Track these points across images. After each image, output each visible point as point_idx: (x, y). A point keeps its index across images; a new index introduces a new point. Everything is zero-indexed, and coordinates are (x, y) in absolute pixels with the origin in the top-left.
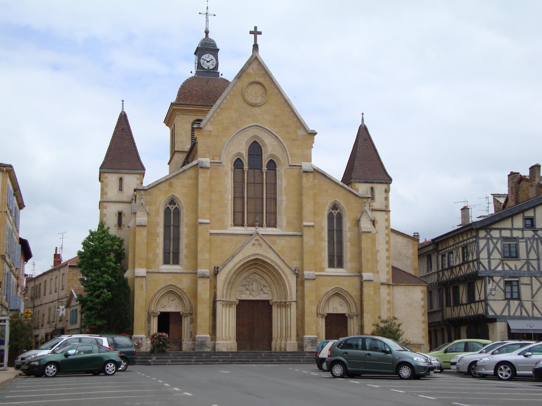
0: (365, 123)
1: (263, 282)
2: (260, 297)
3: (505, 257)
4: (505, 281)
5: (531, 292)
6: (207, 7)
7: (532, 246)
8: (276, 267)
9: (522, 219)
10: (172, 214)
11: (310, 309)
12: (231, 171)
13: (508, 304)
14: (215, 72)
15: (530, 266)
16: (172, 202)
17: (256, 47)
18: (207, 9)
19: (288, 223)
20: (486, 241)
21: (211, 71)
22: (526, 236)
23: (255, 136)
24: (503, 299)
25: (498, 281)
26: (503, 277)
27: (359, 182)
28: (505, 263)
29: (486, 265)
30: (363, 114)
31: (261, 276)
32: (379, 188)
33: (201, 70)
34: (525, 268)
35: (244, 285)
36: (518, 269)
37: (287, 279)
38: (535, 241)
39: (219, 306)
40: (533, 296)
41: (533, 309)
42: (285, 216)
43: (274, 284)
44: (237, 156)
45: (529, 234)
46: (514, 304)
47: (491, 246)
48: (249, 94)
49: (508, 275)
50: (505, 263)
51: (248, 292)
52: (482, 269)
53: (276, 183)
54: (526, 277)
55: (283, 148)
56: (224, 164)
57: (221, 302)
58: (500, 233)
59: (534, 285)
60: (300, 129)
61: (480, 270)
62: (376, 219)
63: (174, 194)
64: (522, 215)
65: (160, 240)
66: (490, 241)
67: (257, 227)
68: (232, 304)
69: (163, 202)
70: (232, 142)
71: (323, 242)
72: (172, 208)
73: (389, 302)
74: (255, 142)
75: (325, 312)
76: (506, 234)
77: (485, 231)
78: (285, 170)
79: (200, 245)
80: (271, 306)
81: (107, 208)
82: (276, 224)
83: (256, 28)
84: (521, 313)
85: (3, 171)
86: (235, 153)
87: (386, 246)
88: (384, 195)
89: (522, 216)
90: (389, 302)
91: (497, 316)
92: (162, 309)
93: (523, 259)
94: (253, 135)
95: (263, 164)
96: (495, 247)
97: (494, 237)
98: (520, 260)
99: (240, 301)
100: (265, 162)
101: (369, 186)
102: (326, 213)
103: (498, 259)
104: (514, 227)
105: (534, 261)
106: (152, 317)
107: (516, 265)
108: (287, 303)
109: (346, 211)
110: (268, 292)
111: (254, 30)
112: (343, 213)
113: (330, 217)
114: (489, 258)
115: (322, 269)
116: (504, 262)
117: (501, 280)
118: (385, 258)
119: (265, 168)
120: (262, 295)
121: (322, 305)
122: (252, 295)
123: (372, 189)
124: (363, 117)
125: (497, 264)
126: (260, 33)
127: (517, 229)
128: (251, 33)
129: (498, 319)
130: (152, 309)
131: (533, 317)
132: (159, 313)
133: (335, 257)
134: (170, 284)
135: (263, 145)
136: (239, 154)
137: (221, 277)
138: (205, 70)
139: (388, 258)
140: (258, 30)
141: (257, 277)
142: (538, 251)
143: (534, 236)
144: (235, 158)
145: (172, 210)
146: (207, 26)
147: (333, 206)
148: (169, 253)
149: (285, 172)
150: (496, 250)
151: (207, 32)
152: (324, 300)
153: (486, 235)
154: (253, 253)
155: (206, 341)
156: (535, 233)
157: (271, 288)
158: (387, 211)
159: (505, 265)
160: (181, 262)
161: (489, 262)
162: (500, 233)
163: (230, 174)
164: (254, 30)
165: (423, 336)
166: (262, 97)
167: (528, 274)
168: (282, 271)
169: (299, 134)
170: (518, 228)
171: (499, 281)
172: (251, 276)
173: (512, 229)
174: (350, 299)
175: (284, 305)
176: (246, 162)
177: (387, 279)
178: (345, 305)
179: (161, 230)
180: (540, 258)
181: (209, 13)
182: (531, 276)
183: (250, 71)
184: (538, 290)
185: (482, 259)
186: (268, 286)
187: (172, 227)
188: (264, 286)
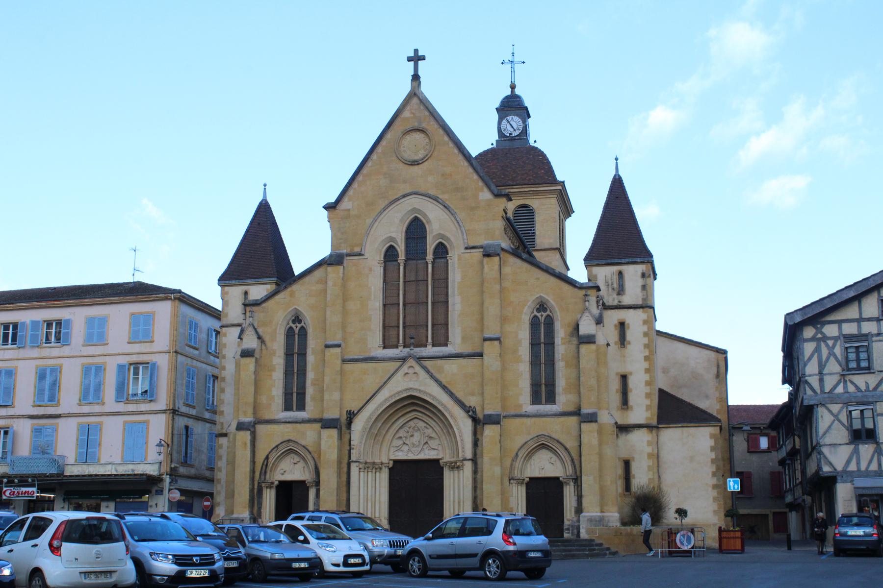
0: (620, 173)
1: (429, 431)
2: (425, 455)
3: (849, 370)
6: (513, 53)
8: (440, 408)
9: (876, 300)
10: (296, 336)
11: (491, 470)
12: (379, 265)
13: (856, 452)
14: (521, 139)
16: (297, 319)
17: (416, 77)
18: (513, 55)
19: (464, 339)
20: (815, 345)
21: (517, 138)
23: (415, 210)
24: (848, 442)
26: (847, 404)
27: (598, 265)
28: (849, 380)
29: (816, 385)
30: (616, 159)
31: (426, 423)
32: (632, 272)
33: (502, 139)
36: (871, 388)
37: (458, 425)
39: (354, 468)
42: (460, 328)
43: (444, 433)
44: (389, 242)
46: (867, 450)
47: (825, 352)
48: (405, 149)
49: (853, 400)
50: (849, 380)
52: (809, 392)
53: (447, 278)
55: (456, 223)
56: (367, 255)
57: (357, 464)
58: (840, 329)
60: (482, 191)
61: (806, 394)
62: (627, 322)
63: (297, 307)
64: (875, 294)
65: (278, 375)
66: (823, 345)
67: (412, 348)
68: (381, 469)
69: (281, 320)
71: (520, 364)
72: (297, 327)
73: (650, 456)
74: (416, 219)
75: (526, 476)
76: (850, 329)
77: (814, 327)
78: (459, 256)
79: (327, 379)
80: (443, 468)
81: (227, 335)
82: (447, 340)
83: (416, 51)
85: (171, 299)
86: (384, 237)
88: (640, 282)
90: (650, 456)
91: (838, 473)
92: (281, 476)
93: (878, 371)
94: (410, 209)
95: (428, 250)
96: (831, 354)
97: (828, 336)
98: (874, 373)
99: (396, 462)
100: (430, 247)
101: (615, 269)
102: (526, 319)
103: (837, 373)
104: (863, 317)
106: (264, 490)
107: (868, 382)
108: (458, 464)
109: (558, 314)
110: (436, 448)
111: (413, 55)
112: (554, 315)
113: (534, 323)
114: (820, 373)
116: (847, 378)
117: (842, 408)
119: (430, 256)
120: (427, 452)
121: (517, 466)
123: (620, 273)
124: (617, 163)
125: (834, 382)
126: (423, 58)
127: (869, 320)
128: (410, 59)
129: (839, 479)
132: (277, 483)
133: (543, 387)
134: (288, 439)
135: (426, 221)
136: (392, 239)
137: (358, 425)
138: (508, 138)
139: (648, 383)
140: (420, 54)
141: (421, 424)
144: (385, 245)
145: (297, 331)
146: (513, 78)
147: (538, 306)
148: (292, 394)
149: (459, 259)
150: (832, 359)
151: (513, 87)
153: (816, 334)
158: (647, 306)
159: (849, 384)
160: (306, 408)
161: (821, 381)
162: (840, 329)
163: (379, 270)
164: (413, 55)
166: (424, 151)
168: (450, 413)
169: (481, 198)
171: (839, 412)
172: (411, 423)
173: (860, 320)
174: (563, 452)
175: (455, 467)
176: (401, 251)
177: (647, 418)
178: (558, 464)
179: (279, 361)
183: (406, 114)
185: (810, 376)
186: (437, 437)
187: (296, 356)
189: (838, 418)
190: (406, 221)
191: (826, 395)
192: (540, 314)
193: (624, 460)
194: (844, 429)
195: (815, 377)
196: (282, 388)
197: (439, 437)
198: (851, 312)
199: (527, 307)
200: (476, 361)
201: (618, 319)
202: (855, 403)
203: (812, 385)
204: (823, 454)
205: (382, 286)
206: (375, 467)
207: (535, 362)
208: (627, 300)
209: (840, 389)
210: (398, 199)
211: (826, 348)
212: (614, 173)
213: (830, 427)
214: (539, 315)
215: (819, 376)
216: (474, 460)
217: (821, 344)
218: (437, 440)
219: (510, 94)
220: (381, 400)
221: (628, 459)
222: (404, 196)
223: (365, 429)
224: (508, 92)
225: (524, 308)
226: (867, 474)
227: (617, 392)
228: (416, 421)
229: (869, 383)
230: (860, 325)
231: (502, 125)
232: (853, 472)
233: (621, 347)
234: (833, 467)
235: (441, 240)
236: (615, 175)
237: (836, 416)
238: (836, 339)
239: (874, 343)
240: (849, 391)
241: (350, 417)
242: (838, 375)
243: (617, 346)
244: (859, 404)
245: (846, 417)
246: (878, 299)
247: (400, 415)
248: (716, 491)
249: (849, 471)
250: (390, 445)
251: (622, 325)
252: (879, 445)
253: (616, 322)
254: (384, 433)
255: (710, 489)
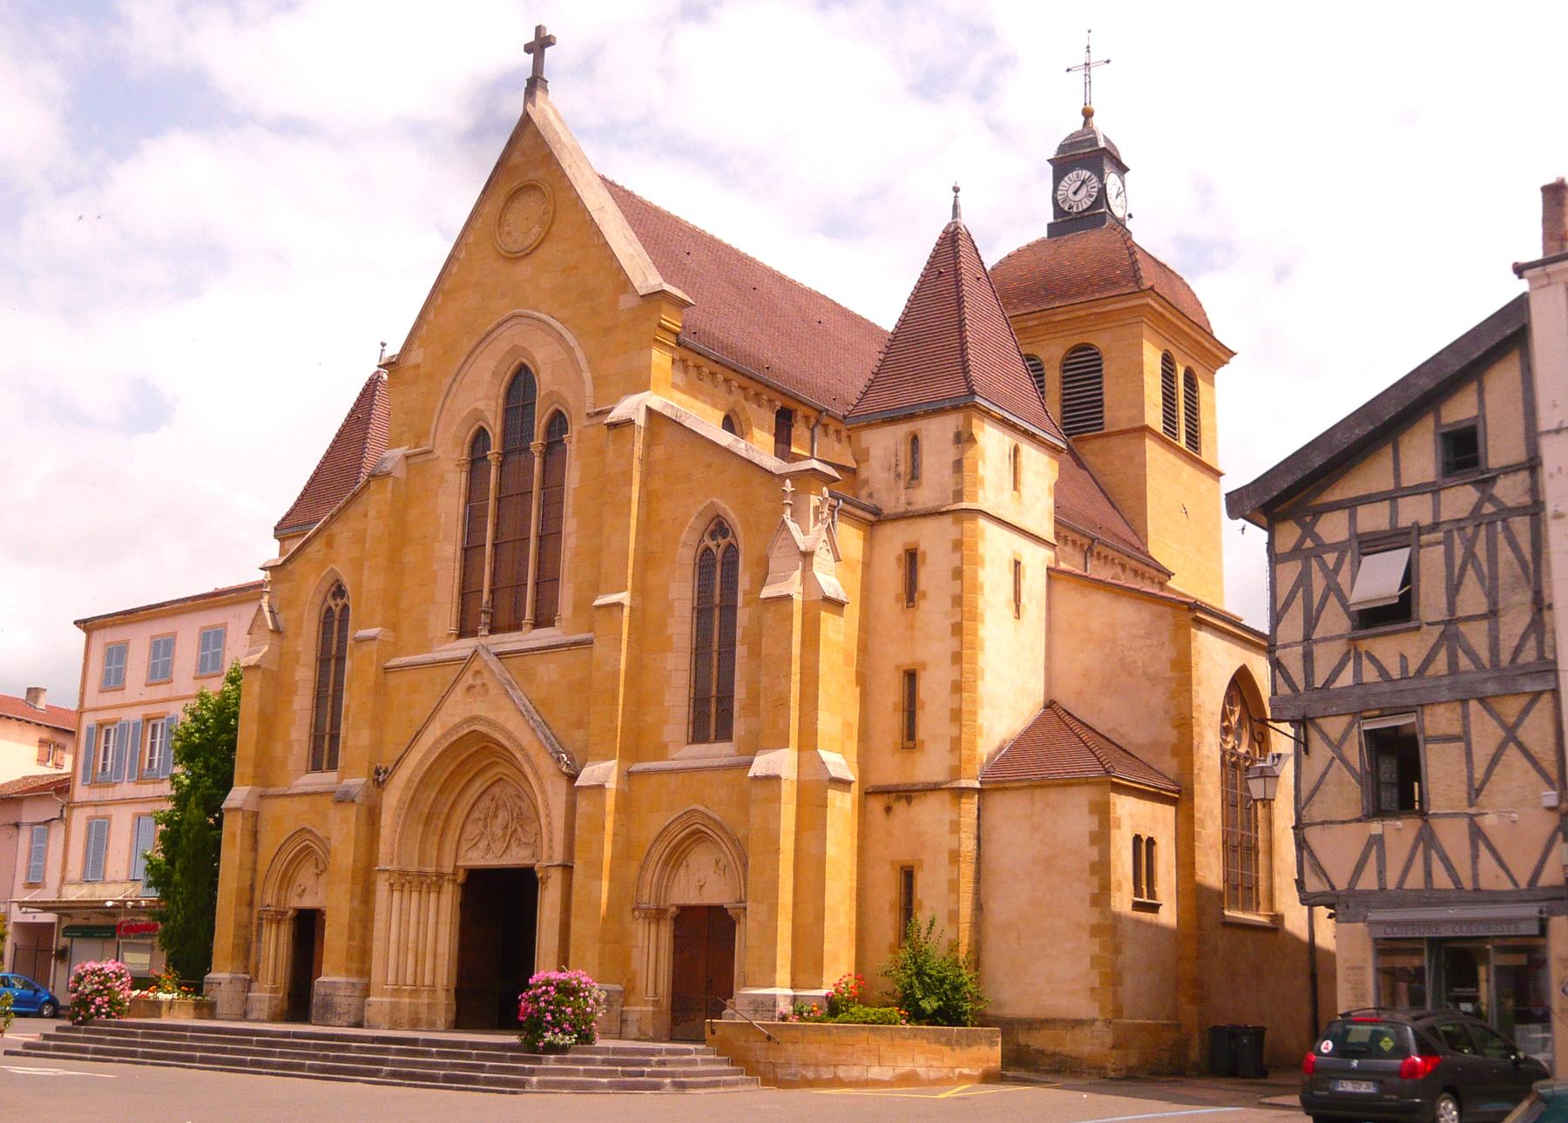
4: (1370, 734)
5: (1465, 773)
6: (1088, 47)
7: (1470, 555)
8: (519, 756)
12: (458, 469)
15: (1460, 653)
16: (339, 591)
18: (1088, 51)
21: (1087, 214)
22: (1445, 515)
24: (1359, 815)
25: (1338, 736)
26: (1358, 715)
28: (1366, 652)
30: (956, 190)
34: (1441, 665)
37: (543, 792)
38: (1483, 532)
39: (382, 887)
40: (1475, 792)
41: (1475, 857)
42: (571, 585)
45: (1460, 499)
46: (1399, 832)
47: (1319, 583)
49: (1373, 704)
50: (1366, 652)
54: (1443, 706)
59: (1474, 739)
62: (922, 547)
64: (1429, 422)
69: (312, 594)
70: (461, 383)
75: (673, 902)
77: (1297, 523)
78: (580, 432)
84: (1428, 874)
86: (466, 411)
87: (951, 644)
88: (951, 454)
89: (1433, 428)
91: (1338, 897)
93: (1428, 624)
98: (1418, 628)
100: (540, 422)
102: (686, 555)
103: (1341, 637)
105: (1474, 624)
113: (705, 563)
114: (1307, 638)
115: (661, 751)
116: (1364, 645)
117: (1351, 726)
118: (948, 688)
123: (915, 440)
127: (1418, 490)
130: (268, 901)
131: (1477, 890)
132: (291, 912)
136: (477, 414)
137: (392, 798)
142: (1494, 577)
143: (1478, 507)
150: (1333, 600)
151: (1088, 114)
152: (655, 856)
153: (1302, 540)
155: (335, 995)
156: (1483, 492)
159: (1366, 662)
161: (1308, 658)
165: (1093, 989)
167: (1452, 688)
170: (1417, 486)
176: (494, 435)
180: (1501, 605)
181: (1093, 59)
182: (1460, 696)
184: (1494, 760)
185: (1285, 646)
189: (1341, 752)
191: (1315, 696)
192: (715, 542)
193: (902, 868)
194: (1353, 781)
195: (1295, 648)
196: (307, 728)
198: (1375, 476)
199: (687, 528)
200: (580, 654)
201: (905, 544)
202: (1377, 713)
203: (1290, 671)
204: (1309, 847)
205: (461, 510)
206: (425, 882)
207: (700, 651)
208: (925, 497)
209: (1346, 679)
211: (1321, 574)
212: (949, 219)
213: (1324, 775)
214: (712, 544)
215: (1304, 647)
216: (567, 868)
217: (1311, 565)
219: (1079, 127)
220: (430, 744)
221: (911, 863)
223: (404, 803)
224: (1077, 124)
225: (681, 532)
226: (1400, 898)
227: (895, 710)
229: (1409, 658)
230: (1397, 506)
231: (1059, 193)
232: (1370, 893)
233: (907, 607)
234: (1329, 881)
235: (556, 405)
236: (949, 225)
237: (1337, 747)
238: (1341, 548)
239: (1423, 551)
240: (1364, 681)
241: (377, 780)
242: (1343, 641)
243: (900, 605)
244: (1388, 712)
245: (1358, 748)
246: (1435, 434)
248: (1097, 940)
249: (1361, 892)
251: (912, 558)
252: (1426, 821)
253: (900, 550)
255: (1086, 936)
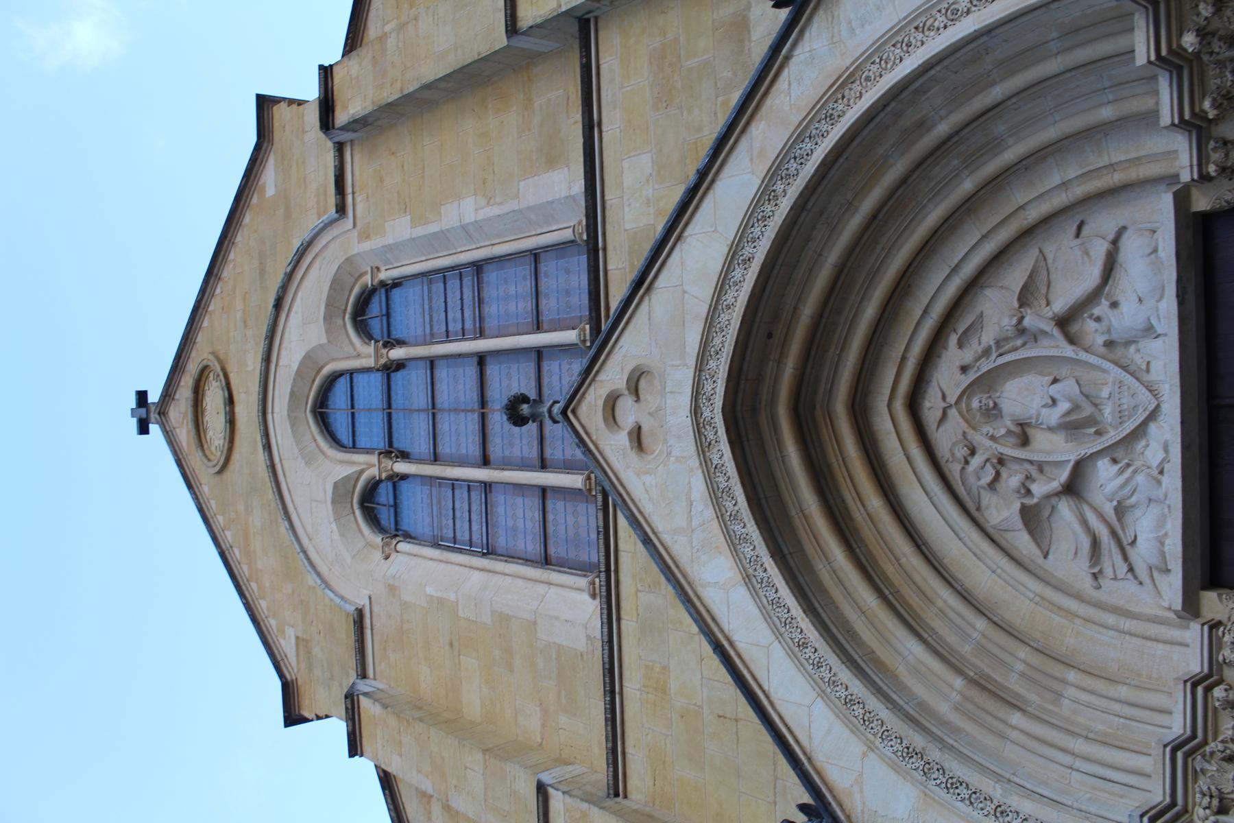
35: (1032, 518)
37: (878, 54)
51: (1105, 475)
110: (1100, 249)
122: (1140, 431)
154: (688, 446)
157: (1046, 221)
172: (946, 439)
188: (1025, 297)
190: (318, 446)
197: (1027, 234)
210: (272, 467)
218: (1050, 250)
222: (268, 447)
228: (931, 406)
247: (875, 502)
250: (1078, 597)
254: (981, 624)
